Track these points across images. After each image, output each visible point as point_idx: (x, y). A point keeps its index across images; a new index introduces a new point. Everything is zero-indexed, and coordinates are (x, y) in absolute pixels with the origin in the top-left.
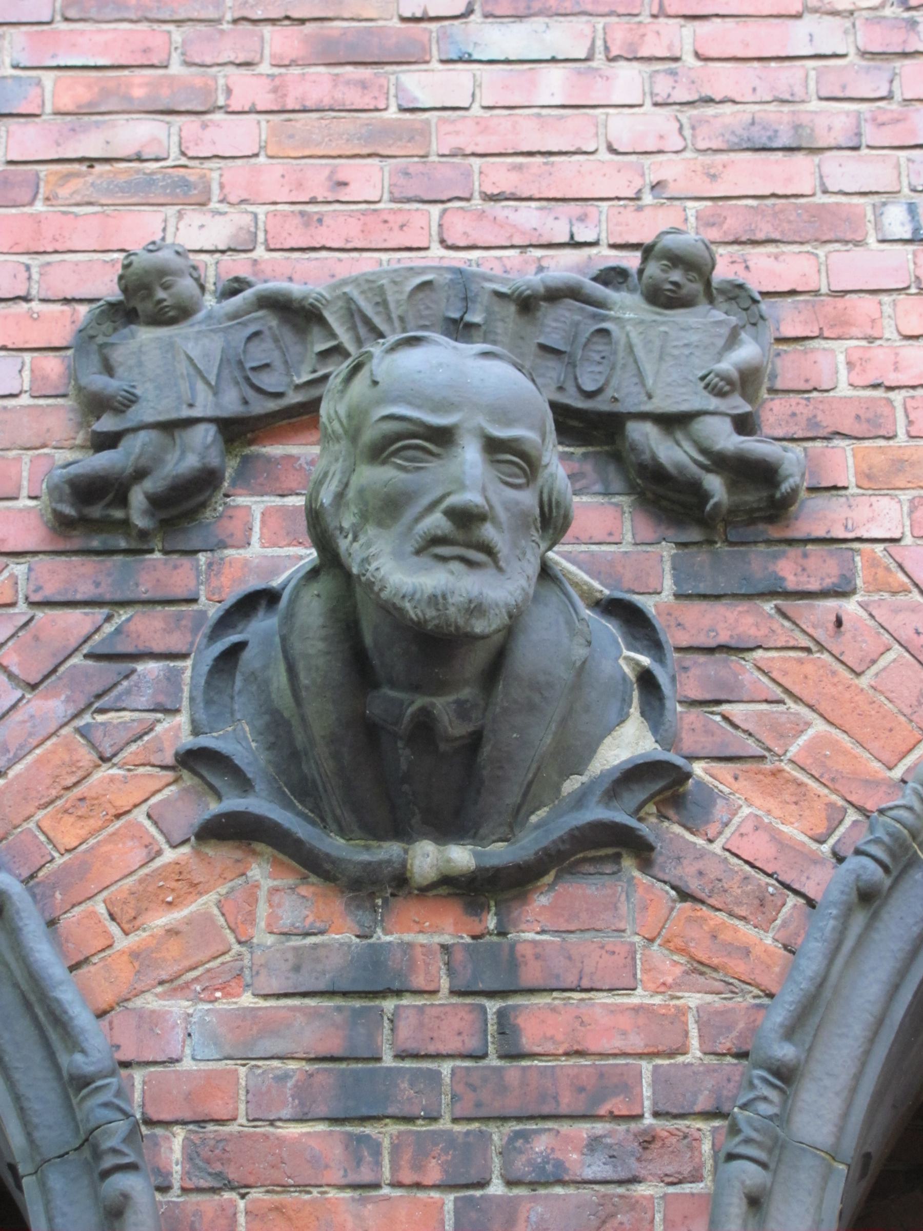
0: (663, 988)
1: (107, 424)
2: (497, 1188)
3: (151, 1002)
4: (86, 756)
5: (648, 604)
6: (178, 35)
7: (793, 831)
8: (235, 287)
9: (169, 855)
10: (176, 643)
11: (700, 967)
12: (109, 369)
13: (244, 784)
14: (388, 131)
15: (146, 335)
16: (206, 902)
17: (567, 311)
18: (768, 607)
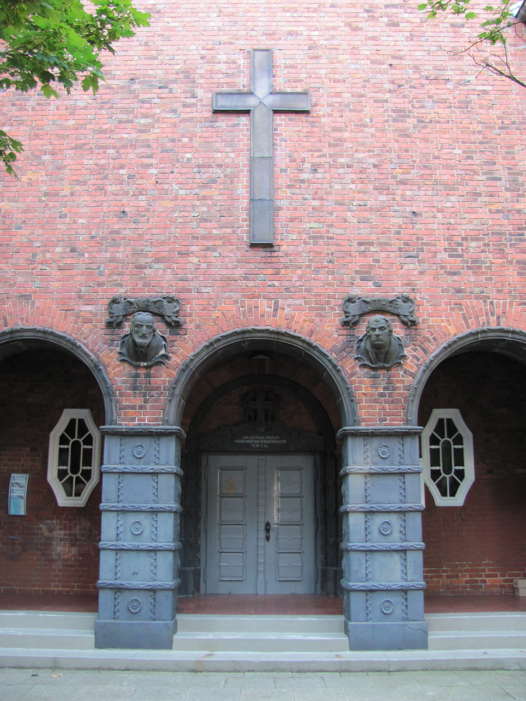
0: (164, 377)
1: (111, 316)
2: (148, 397)
3: (115, 378)
4: (109, 352)
5: (166, 336)
6: (120, 265)
7: (178, 361)
8: (125, 299)
9: (118, 363)
10: (118, 339)
11: (168, 375)
12: (111, 309)
13: (124, 356)
14: (142, 278)
15: (116, 305)
16: (121, 368)
17: (160, 303)
18: (178, 336)
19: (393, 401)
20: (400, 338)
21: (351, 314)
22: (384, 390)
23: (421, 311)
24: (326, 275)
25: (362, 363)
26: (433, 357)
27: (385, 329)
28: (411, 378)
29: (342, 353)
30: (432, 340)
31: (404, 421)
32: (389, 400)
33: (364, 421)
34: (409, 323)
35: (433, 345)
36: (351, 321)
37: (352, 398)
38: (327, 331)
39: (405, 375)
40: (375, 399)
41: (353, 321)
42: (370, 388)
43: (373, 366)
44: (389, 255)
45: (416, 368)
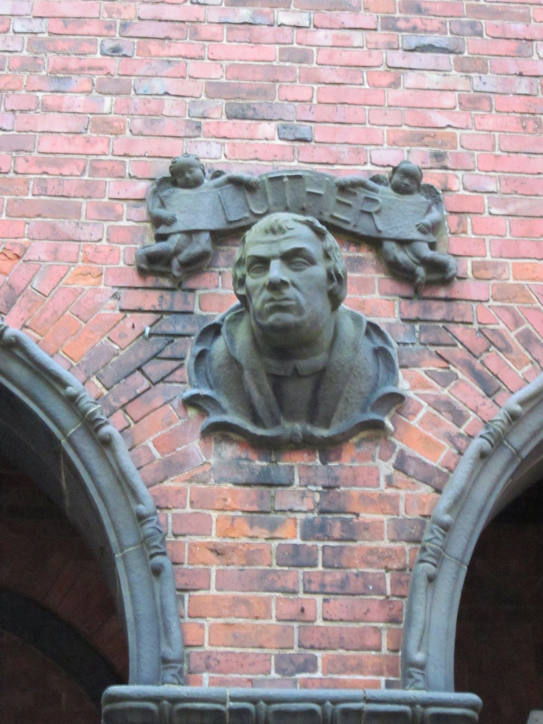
19: (345, 581)
20: (383, 328)
21: (179, 226)
22: (304, 538)
23: (470, 235)
24: (95, 93)
25: (215, 418)
26: (522, 403)
27: (312, 262)
28: (425, 490)
29: (130, 380)
30: (517, 345)
31: (392, 671)
32: (328, 579)
33: (208, 668)
34: (421, 271)
35: (519, 363)
36: (177, 252)
37: (158, 559)
38: (77, 293)
39: (399, 476)
40: (265, 574)
41: (182, 257)
42: (246, 528)
43: (260, 432)
44: (348, 38)
45: (448, 449)
